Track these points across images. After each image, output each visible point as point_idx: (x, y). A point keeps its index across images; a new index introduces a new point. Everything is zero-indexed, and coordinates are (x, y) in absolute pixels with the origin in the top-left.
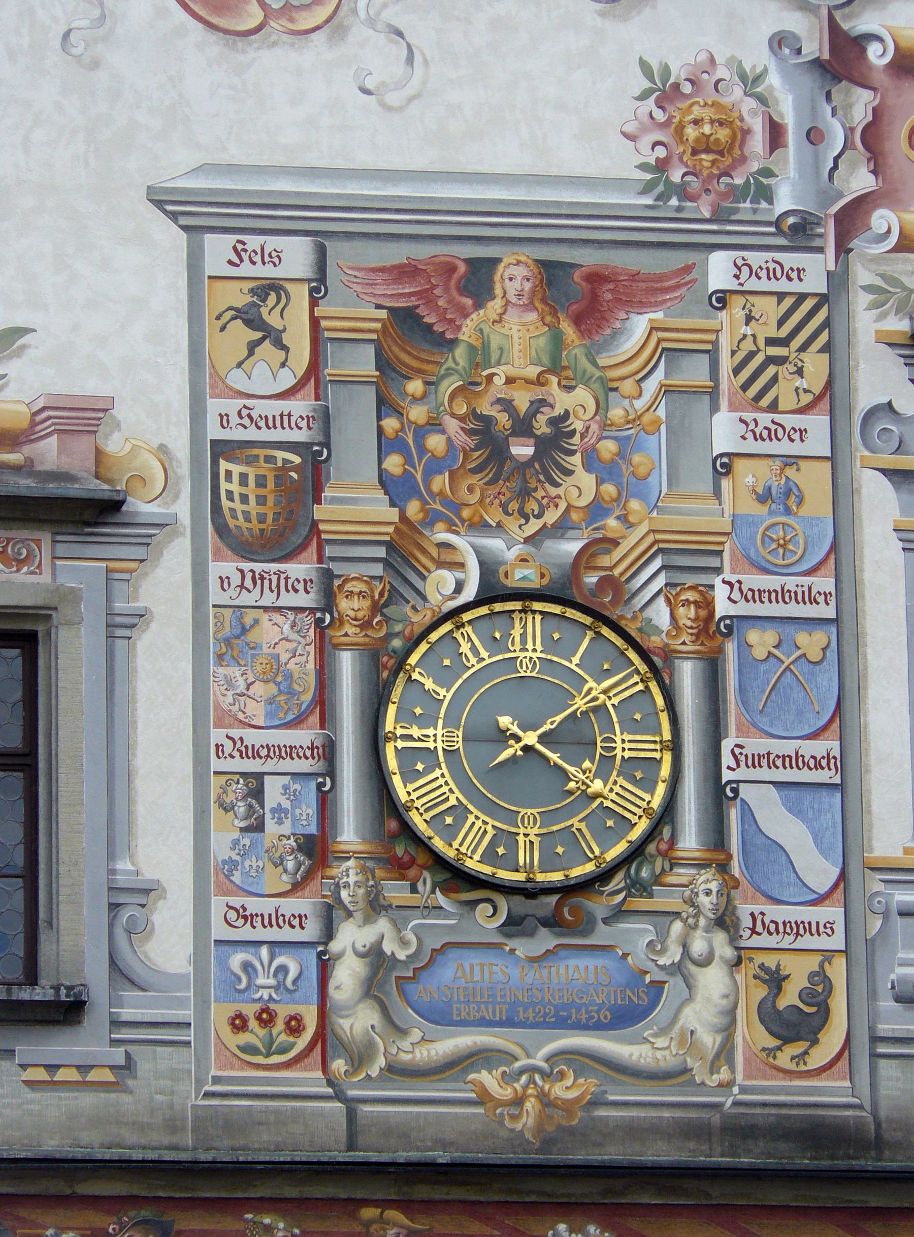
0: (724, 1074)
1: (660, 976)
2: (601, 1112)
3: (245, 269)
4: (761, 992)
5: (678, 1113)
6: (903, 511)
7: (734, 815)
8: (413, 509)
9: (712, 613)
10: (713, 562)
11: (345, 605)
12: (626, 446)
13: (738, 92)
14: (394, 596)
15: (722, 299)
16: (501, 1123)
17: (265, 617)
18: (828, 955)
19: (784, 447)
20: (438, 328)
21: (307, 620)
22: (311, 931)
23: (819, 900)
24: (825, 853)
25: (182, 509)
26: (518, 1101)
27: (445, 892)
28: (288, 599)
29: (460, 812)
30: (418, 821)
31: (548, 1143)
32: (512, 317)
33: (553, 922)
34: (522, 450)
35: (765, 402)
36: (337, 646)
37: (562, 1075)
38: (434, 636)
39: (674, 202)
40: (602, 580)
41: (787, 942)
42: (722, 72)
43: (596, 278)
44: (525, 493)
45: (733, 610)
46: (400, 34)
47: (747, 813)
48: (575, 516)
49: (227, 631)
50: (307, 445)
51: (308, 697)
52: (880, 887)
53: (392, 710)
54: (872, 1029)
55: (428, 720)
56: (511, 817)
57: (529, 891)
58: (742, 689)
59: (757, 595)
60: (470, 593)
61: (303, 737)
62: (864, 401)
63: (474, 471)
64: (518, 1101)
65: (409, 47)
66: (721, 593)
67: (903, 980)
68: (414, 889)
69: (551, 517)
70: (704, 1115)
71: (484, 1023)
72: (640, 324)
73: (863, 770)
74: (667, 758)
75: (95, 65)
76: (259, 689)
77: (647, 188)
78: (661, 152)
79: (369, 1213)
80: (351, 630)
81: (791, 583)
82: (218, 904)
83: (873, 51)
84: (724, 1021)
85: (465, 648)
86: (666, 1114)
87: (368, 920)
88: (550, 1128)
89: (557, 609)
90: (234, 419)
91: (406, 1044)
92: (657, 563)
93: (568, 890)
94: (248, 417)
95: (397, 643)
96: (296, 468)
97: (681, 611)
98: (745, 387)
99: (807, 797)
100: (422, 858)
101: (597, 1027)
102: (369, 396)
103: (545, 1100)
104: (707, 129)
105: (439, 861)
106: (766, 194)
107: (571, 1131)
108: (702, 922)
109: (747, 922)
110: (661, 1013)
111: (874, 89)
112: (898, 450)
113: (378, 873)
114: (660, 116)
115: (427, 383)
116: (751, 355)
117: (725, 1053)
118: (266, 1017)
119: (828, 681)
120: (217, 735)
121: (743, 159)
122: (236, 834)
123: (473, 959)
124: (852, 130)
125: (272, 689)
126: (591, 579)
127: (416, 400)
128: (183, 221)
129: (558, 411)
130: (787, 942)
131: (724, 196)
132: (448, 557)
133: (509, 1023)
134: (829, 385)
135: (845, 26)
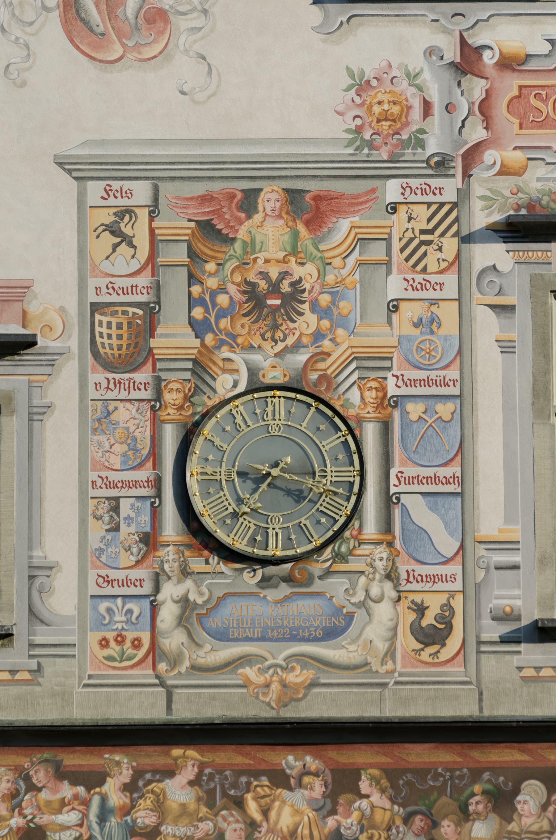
0: (390, 666)
1: (352, 609)
3: (112, 201)
4: (412, 616)
6: (501, 330)
7: (397, 512)
8: (209, 339)
9: (385, 395)
10: (387, 364)
11: (168, 397)
13: (405, 84)
14: (197, 390)
15: (393, 208)
16: (257, 698)
17: (120, 405)
18: (452, 594)
19: (430, 294)
20: (225, 232)
21: (146, 406)
22: (147, 589)
23: (448, 561)
24: (451, 534)
25: (73, 343)
26: (268, 685)
28: (135, 395)
33: (288, 579)
35: (419, 268)
36: (163, 421)
37: (293, 669)
39: (366, 151)
40: (321, 377)
41: (428, 586)
43: (318, 198)
44: (275, 327)
45: (398, 392)
46: (204, 58)
47: (405, 511)
48: (305, 340)
49: (99, 414)
50: (147, 304)
51: (145, 452)
52: (484, 553)
54: (477, 636)
58: (403, 438)
59: (413, 383)
60: (242, 388)
61: (144, 475)
63: (245, 315)
64: (268, 685)
65: (209, 65)
66: (391, 382)
68: (207, 562)
69: (290, 341)
71: (248, 639)
75: (24, 84)
77: (350, 143)
78: (358, 122)
80: (171, 411)
81: (433, 375)
82: (92, 575)
83: (487, 55)
84: (390, 634)
87: (179, 581)
90: (104, 290)
91: (201, 653)
92: (353, 366)
94: (111, 288)
96: (140, 318)
97: (367, 394)
98: (407, 260)
99: (441, 501)
101: (315, 640)
102: (184, 272)
103: (284, 685)
104: (386, 107)
106: (421, 144)
108: (377, 576)
109: (404, 576)
110: (352, 631)
111: (487, 78)
112: (499, 293)
113: (187, 553)
114: (358, 100)
115: (218, 264)
116: (411, 240)
117: (390, 653)
121: (407, 124)
122: (103, 533)
124: (473, 103)
125: (125, 448)
126: (314, 376)
127: (211, 275)
128: (75, 174)
129: (296, 277)
130: (428, 586)
131: (396, 146)
132: (229, 366)
133: (263, 639)
134: (458, 256)
135: (470, 41)
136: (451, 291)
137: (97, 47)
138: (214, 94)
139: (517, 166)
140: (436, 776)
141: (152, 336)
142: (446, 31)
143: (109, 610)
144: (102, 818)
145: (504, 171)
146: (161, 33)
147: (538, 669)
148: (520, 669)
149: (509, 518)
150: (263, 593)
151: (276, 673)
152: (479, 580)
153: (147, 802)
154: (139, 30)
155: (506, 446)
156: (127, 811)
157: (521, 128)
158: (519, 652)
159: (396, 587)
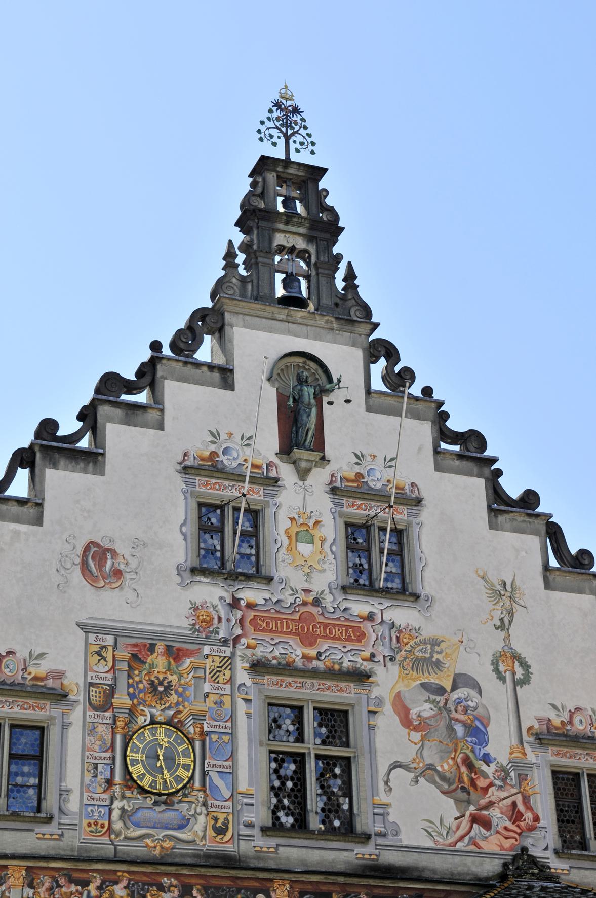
0: (204, 842)
1: (189, 817)
2: (175, 850)
3: (98, 642)
4: (213, 822)
5: (193, 852)
7: (207, 779)
8: (135, 701)
9: (203, 730)
10: (204, 718)
11: (118, 723)
13: (212, 609)
14: (130, 722)
15: (207, 656)
16: (151, 852)
17: (100, 725)
18: (228, 814)
19: (220, 692)
20: (142, 659)
21: (110, 726)
22: (108, 803)
24: (228, 789)
25: (81, 698)
26: (155, 847)
27: (140, 794)
28: (105, 721)
29: (144, 775)
30: (134, 776)
31: (162, 857)
32: (159, 657)
33: (165, 803)
34: (161, 689)
35: (216, 681)
36: (116, 733)
37: (166, 841)
38: (139, 732)
39: (197, 633)
40: (178, 721)
41: (219, 810)
42: (208, 604)
43: (179, 650)
44: (161, 699)
47: (210, 778)
48: (173, 705)
49: (90, 728)
50: (111, 685)
51: (109, 745)
52: (241, 798)
53: (129, 749)
54: (238, 832)
55: (137, 752)
56: (156, 777)
57: (160, 794)
58: (210, 749)
59: (214, 726)
60: (148, 722)
61: (108, 755)
62: (238, 682)
63: (150, 693)
64: (155, 847)
66: (205, 725)
67: (245, 820)
68: (132, 794)
69: (167, 705)
70: (199, 852)
72: (188, 661)
73: (237, 770)
74: (193, 764)
75: (65, 592)
76: (98, 743)
77: (191, 630)
78: (194, 622)
79: (119, 874)
80: (120, 729)
81: (221, 724)
82: (85, 795)
83: (242, 602)
84: (203, 829)
85: (146, 735)
86: (190, 851)
87: (121, 801)
88: (163, 854)
89: (168, 727)
90: (94, 678)
91: (129, 832)
92: (191, 717)
93: (168, 794)
95: (130, 733)
96: (108, 690)
97: (196, 729)
98: (212, 677)
99: (224, 775)
100: (135, 785)
103: (162, 847)
104: (204, 617)
106: (217, 633)
107: (167, 855)
108: (200, 804)
109: (210, 805)
112: (246, 694)
113: (124, 789)
114: (194, 613)
115: (139, 672)
116: (213, 670)
117: (204, 837)
118: (96, 824)
119: (229, 748)
120: (87, 753)
121: (212, 625)
122: (91, 778)
123: (146, 811)
125: (100, 743)
126: (176, 720)
127: (136, 675)
128: (84, 630)
129: (169, 680)
130: (219, 810)
131: (208, 633)
132: (143, 713)
133: (154, 827)
134: (231, 678)
135: (236, 596)
136: (228, 692)
137: (95, 581)
138: (139, 605)
139: (253, 645)
140: (223, 890)
141: (113, 698)
142: (227, 591)
143: (92, 811)
145: (248, 647)
146: (120, 578)
147: (261, 848)
148: (255, 847)
149: (250, 784)
150: (155, 808)
151: (159, 842)
152: (239, 809)
154: (111, 577)
155: (249, 755)
157: (254, 631)
158: (254, 840)
159: (207, 809)
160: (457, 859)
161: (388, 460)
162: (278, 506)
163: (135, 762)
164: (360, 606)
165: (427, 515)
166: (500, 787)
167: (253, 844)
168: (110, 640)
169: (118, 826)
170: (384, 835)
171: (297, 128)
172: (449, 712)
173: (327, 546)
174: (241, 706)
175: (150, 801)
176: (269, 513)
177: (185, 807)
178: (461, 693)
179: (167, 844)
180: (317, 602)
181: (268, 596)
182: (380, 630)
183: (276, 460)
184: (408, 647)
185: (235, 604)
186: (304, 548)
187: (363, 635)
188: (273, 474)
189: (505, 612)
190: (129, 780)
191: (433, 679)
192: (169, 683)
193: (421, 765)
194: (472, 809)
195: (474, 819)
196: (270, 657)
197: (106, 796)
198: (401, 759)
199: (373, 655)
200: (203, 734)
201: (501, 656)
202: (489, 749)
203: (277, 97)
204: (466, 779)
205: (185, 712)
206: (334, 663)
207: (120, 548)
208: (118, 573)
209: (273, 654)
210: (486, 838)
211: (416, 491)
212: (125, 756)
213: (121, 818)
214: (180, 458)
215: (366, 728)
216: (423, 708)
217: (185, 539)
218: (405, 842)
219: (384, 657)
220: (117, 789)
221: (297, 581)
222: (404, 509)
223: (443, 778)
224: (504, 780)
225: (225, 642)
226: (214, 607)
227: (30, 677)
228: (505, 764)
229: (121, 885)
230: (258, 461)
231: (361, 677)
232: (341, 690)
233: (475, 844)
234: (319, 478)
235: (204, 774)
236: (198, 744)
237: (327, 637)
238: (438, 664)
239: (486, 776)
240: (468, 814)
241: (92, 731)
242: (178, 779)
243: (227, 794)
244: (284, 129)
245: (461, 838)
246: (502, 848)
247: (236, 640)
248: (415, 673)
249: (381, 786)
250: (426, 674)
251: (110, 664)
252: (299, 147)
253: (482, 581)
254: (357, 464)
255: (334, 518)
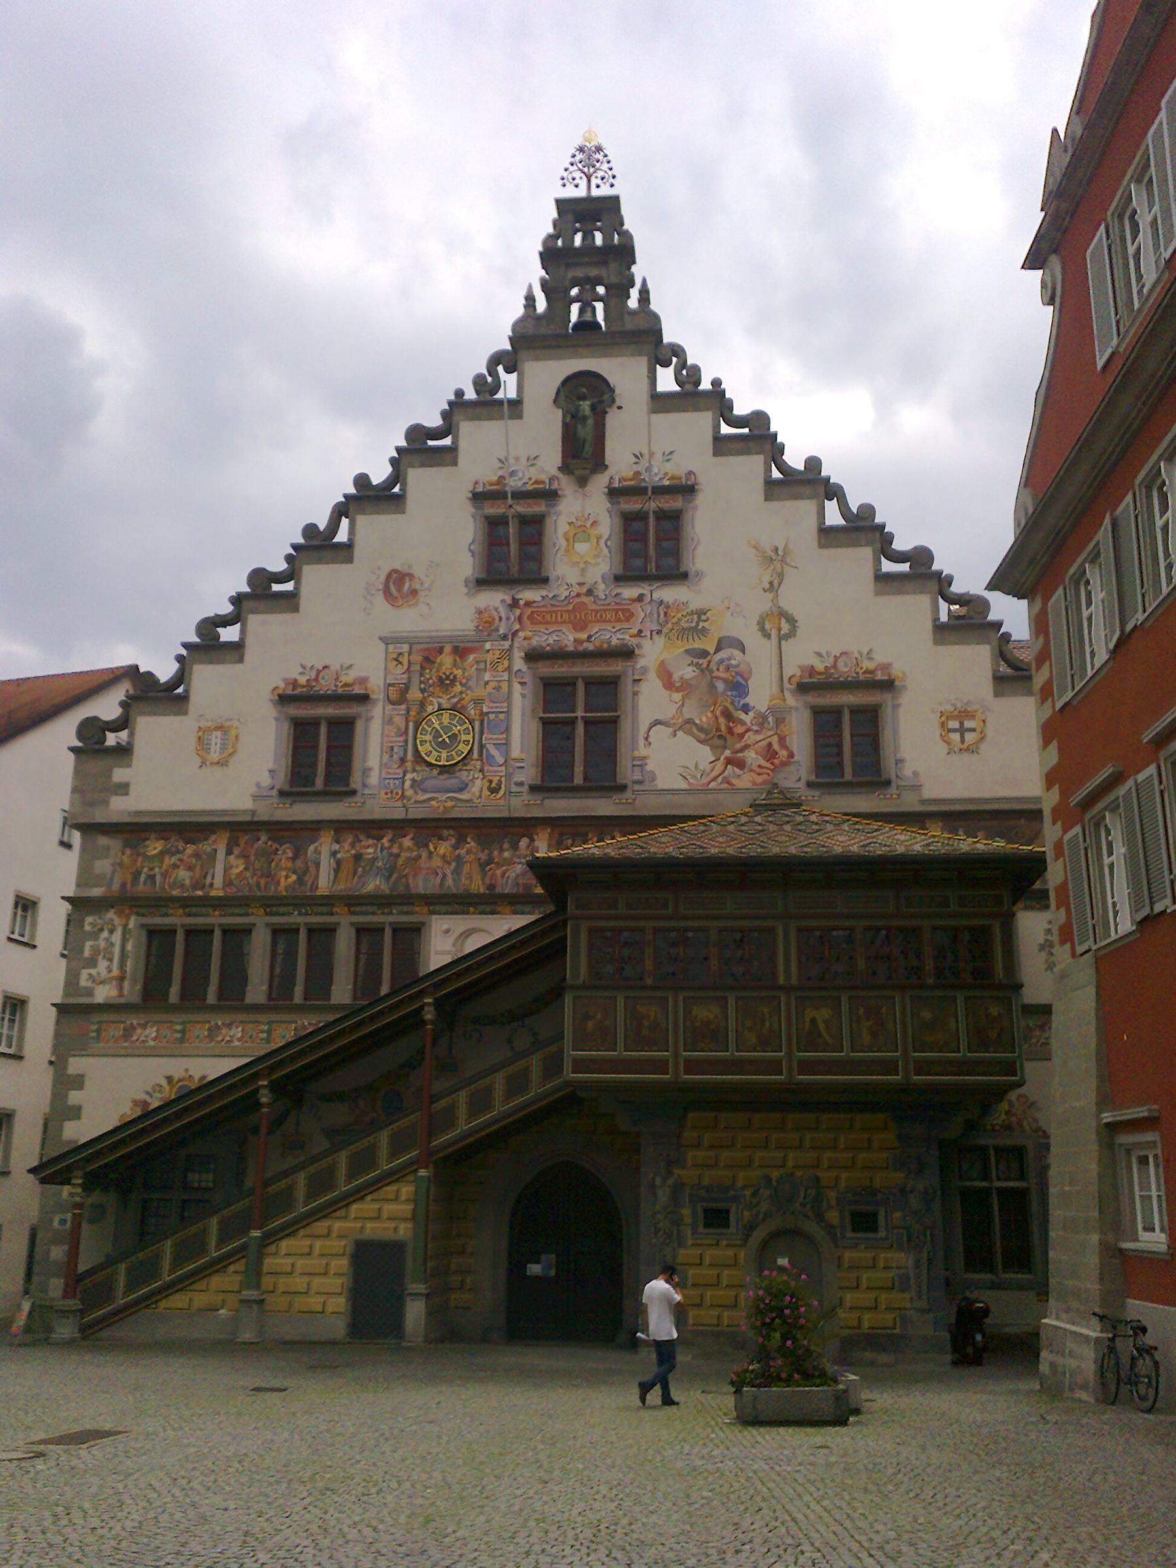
8: (426, 694)
11: (411, 713)
12: (468, 680)
15: (488, 651)
18: (501, 777)
25: (381, 697)
26: (439, 807)
29: (431, 752)
33: (447, 772)
44: (447, 690)
47: (487, 750)
61: (402, 739)
62: (516, 668)
71: (434, 792)
72: (471, 657)
82: (384, 771)
93: (450, 765)
101: (454, 792)
105: (426, 761)
106: (498, 631)
117: (480, 797)
144: (382, 850)
149: (522, 751)
153: (396, 846)
156: (390, 848)
160: (710, 797)
161: (667, 453)
162: (558, 514)
163: (423, 742)
164: (629, 592)
165: (700, 499)
166: (757, 732)
167: (522, 798)
168: (406, 647)
169: (409, 793)
170: (640, 782)
171: (598, 165)
172: (711, 671)
173: (602, 542)
174: (517, 687)
175: (435, 772)
176: (549, 523)
177: (465, 773)
178: (722, 654)
179: (449, 804)
180: (590, 592)
181: (544, 593)
182: (648, 609)
183: (560, 475)
184: (675, 620)
185: (515, 603)
186: (581, 547)
187: (633, 615)
188: (555, 486)
189: (775, 575)
190: (419, 758)
191: (697, 645)
192: (455, 676)
193: (680, 720)
194: (727, 753)
195: (729, 761)
196: (544, 645)
197: (400, 771)
198: (661, 717)
199: (640, 631)
200: (482, 714)
201: (767, 615)
202: (747, 700)
203: (579, 142)
204: (723, 728)
205: (468, 699)
206: (603, 643)
207: (418, 571)
208: (414, 593)
209: (548, 642)
210: (739, 776)
211: (693, 477)
212: (415, 739)
213: (412, 787)
214: (471, 488)
215: (630, 694)
216: (686, 671)
217: (473, 555)
218: (660, 787)
219: (651, 631)
220: (409, 765)
221: (572, 576)
222: (680, 498)
223: (700, 729)
224: (761, 725)
225: (504, 638)
226: (496, 609)
227: (341, 684)
228: (763, 711)
229: (408, 838)
230: (543, 477)
231: (627, 653)
232: (609, 665)
233: (729, 783)
234: (600, 482)
235: (482, 746)
236: (477, 724)
237: (598, 621)
238: (704, 631)
239: (743, 723)
240: (722, 758)
241: (390, 721)
242: (459, 753)
243: (501, 760)
244: (586, 170)
245: (714, 779)
246: (754, 783)
247: (515, 634)
248: (680, 642)
249: (642, 742)
250: (691, 640)
251: (406, 667)
252: (599, 181)
253: (754, 551)
254: (636, 463)
255: (610, 517)
